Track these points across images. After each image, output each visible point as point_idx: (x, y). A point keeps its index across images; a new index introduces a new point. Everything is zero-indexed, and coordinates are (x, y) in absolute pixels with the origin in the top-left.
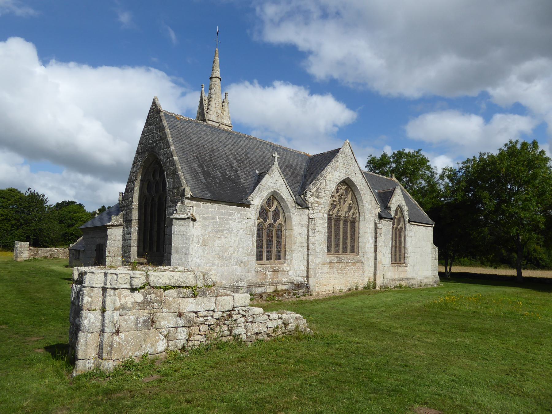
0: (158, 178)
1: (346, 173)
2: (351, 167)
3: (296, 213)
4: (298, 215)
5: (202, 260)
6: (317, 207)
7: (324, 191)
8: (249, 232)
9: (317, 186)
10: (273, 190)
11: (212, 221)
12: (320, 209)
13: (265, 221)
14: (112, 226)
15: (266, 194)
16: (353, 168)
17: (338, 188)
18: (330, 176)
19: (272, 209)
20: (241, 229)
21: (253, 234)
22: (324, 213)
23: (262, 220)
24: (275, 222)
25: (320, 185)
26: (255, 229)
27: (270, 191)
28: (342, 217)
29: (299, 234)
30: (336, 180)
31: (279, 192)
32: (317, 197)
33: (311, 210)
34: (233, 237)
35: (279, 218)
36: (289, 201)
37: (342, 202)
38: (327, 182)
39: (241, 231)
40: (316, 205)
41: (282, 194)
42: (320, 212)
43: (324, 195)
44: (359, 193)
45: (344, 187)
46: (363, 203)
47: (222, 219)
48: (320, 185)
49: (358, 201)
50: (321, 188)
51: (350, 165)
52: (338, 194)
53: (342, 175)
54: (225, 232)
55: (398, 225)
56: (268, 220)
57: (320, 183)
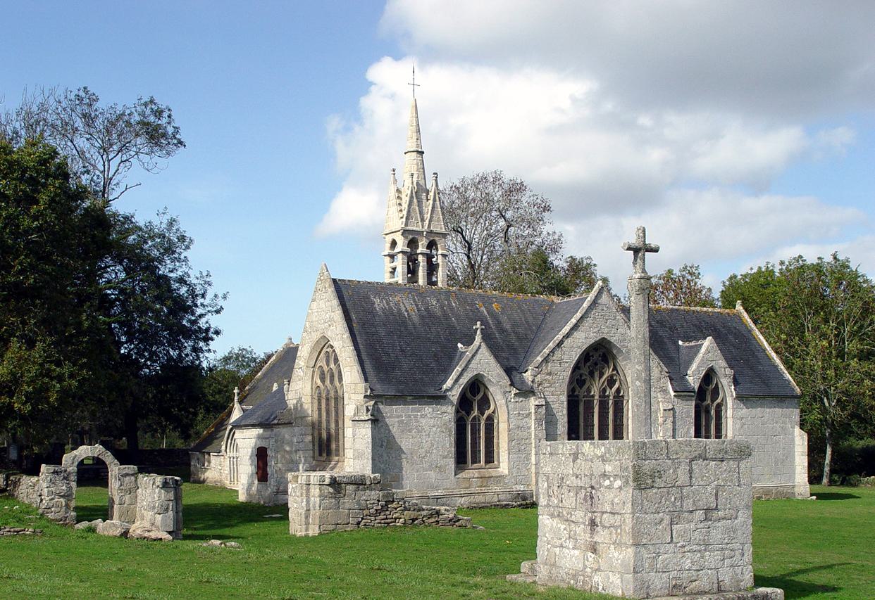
0: (332, 366)
5: (387, 466)
10: (475, 373)
11: (397, 419)
13: (468, 414)
14: (278, 424)
16: (613, 322)
17: (588, 354)
19: (479, 396)
20: (434, 426)
21: (450, 431)
23: (464, 412)
26: (453, 425)
34: (424, 437)
39: (434, 429)
41: (490, 377)
47: (410, 416)
51: (607, 317)
52: (588, 364)
54: (413, 432)
55: (713, 401)
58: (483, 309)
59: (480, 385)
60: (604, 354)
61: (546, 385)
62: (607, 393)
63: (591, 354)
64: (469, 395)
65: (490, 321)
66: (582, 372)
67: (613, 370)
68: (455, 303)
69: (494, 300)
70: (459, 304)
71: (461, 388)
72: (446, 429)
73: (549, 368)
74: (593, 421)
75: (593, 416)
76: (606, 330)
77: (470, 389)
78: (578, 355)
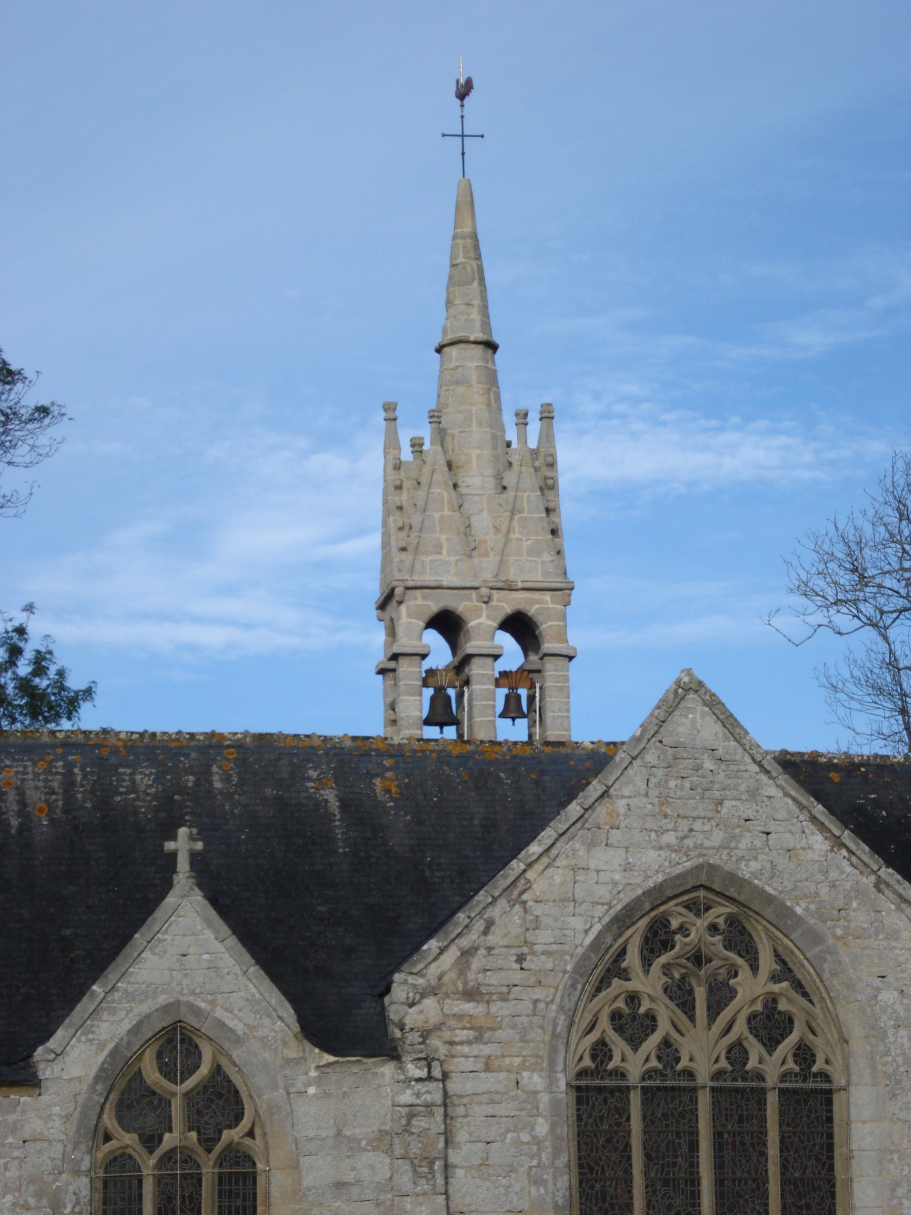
1: (689, 842)
2: (727, 804)
3: (312, 1090)
4: (326, 1095)
6: (469, 1043)
7: (520, 959)
8: (32, 1201)
9: (465, 942)
10: (163, 999)
12: (487, 1050)
13: (151, 1141)
15: (127, 1025)
18: (557, 876)
22: (523, 1067)
23: (130, 1139)
24: (208, 1143)
25: (486, 932)
27: (145, 1008)
28: (703, 1077)
29: (340, 1185)
30: (603, 892)
31: (203, 1005)
32: (471, 994)
33: (410, 1066)
35: (239, 1117)
36: (263, 1040)
37: (700, 994)
38: (538, 910)
40: (462, 1035)
41: (219, 1013)
42: (488, 1068)
43: (518, 977)
44: (816, 938)
45: (719, 913)
46: (850, 985)
48: (486, 932)
49: (826, 975)
50: (490, 949)
51: (717, 794)
52: (663, 959)
53: (652, 857)
56: (167, 1136)
57: (480, 925)
58: (330, 795)
59: (198, 1041)
60: (732, 920)
61: (462, 1035)
62: (752, 1064)
63: (675, 924)
64: (153, 1075)
65: (339, 834)
66: (633, 985)
67: (775, 978)
68: (227, 779)
69: (387, 763)
70: (242, 782)
71: (106, 1052)
72: (38, 1195)
73: (471, 976)
74: (694, 1165)
75: (694, 1146)
76: (717, 838)
77: (160, 1056)
78: (598, 927)
